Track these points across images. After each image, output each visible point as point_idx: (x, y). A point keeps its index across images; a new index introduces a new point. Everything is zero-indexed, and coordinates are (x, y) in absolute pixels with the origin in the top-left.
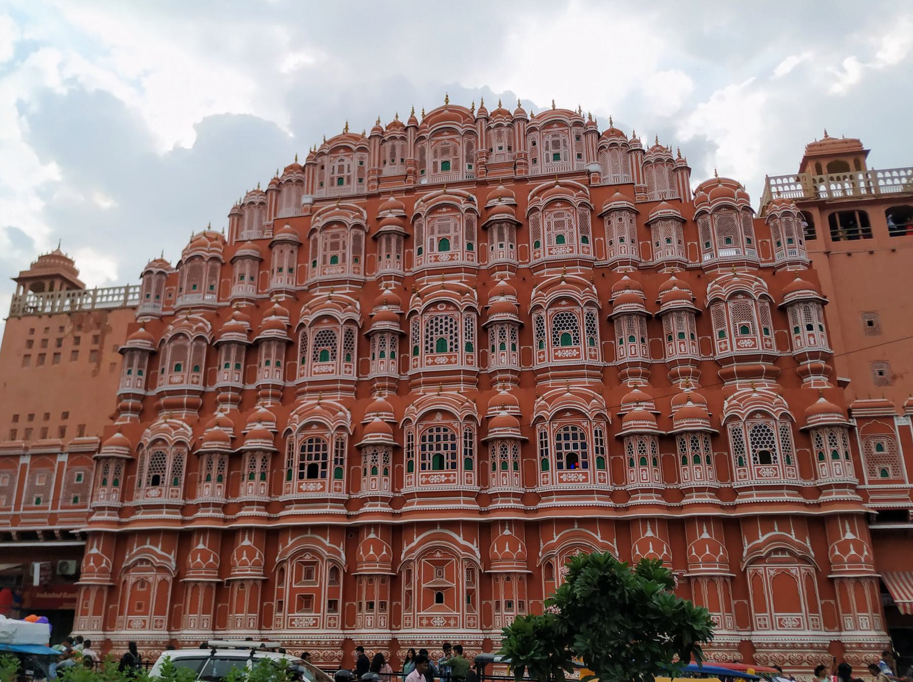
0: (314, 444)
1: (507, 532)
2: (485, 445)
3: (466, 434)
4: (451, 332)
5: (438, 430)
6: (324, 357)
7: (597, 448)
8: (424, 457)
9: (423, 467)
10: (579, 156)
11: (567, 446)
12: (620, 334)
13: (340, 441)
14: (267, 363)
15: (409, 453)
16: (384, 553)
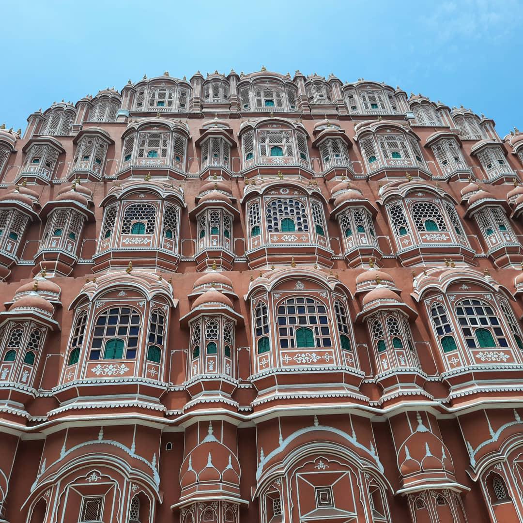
0: (119, 315)
1: (422, 428)
2: (361, 325)
3: (337, 307)
4: (298, 213)
5: (300, 300)
6: (138, 228)
7: (510, 324)
8: (283, 332)
9: (284, 344)
10: (394, 108)
11: (473, 321)
12: (486, 223)
13: (158, 314)
14: (58, 232)
15: (259, 332)
16: (230, 466)
